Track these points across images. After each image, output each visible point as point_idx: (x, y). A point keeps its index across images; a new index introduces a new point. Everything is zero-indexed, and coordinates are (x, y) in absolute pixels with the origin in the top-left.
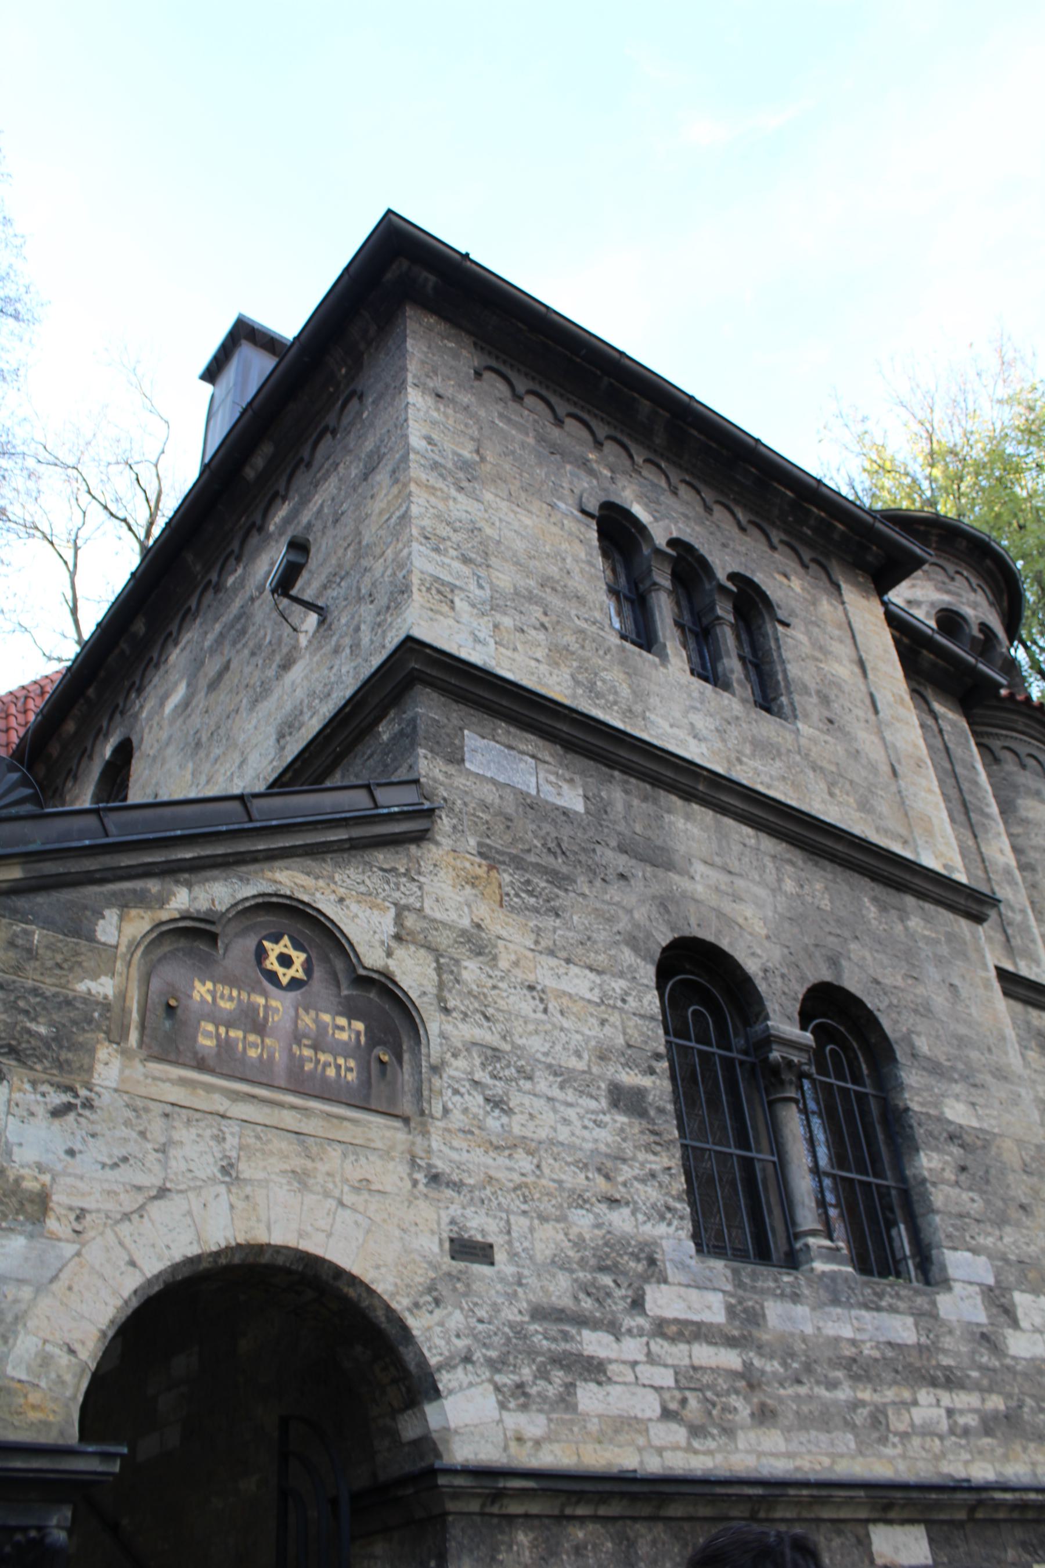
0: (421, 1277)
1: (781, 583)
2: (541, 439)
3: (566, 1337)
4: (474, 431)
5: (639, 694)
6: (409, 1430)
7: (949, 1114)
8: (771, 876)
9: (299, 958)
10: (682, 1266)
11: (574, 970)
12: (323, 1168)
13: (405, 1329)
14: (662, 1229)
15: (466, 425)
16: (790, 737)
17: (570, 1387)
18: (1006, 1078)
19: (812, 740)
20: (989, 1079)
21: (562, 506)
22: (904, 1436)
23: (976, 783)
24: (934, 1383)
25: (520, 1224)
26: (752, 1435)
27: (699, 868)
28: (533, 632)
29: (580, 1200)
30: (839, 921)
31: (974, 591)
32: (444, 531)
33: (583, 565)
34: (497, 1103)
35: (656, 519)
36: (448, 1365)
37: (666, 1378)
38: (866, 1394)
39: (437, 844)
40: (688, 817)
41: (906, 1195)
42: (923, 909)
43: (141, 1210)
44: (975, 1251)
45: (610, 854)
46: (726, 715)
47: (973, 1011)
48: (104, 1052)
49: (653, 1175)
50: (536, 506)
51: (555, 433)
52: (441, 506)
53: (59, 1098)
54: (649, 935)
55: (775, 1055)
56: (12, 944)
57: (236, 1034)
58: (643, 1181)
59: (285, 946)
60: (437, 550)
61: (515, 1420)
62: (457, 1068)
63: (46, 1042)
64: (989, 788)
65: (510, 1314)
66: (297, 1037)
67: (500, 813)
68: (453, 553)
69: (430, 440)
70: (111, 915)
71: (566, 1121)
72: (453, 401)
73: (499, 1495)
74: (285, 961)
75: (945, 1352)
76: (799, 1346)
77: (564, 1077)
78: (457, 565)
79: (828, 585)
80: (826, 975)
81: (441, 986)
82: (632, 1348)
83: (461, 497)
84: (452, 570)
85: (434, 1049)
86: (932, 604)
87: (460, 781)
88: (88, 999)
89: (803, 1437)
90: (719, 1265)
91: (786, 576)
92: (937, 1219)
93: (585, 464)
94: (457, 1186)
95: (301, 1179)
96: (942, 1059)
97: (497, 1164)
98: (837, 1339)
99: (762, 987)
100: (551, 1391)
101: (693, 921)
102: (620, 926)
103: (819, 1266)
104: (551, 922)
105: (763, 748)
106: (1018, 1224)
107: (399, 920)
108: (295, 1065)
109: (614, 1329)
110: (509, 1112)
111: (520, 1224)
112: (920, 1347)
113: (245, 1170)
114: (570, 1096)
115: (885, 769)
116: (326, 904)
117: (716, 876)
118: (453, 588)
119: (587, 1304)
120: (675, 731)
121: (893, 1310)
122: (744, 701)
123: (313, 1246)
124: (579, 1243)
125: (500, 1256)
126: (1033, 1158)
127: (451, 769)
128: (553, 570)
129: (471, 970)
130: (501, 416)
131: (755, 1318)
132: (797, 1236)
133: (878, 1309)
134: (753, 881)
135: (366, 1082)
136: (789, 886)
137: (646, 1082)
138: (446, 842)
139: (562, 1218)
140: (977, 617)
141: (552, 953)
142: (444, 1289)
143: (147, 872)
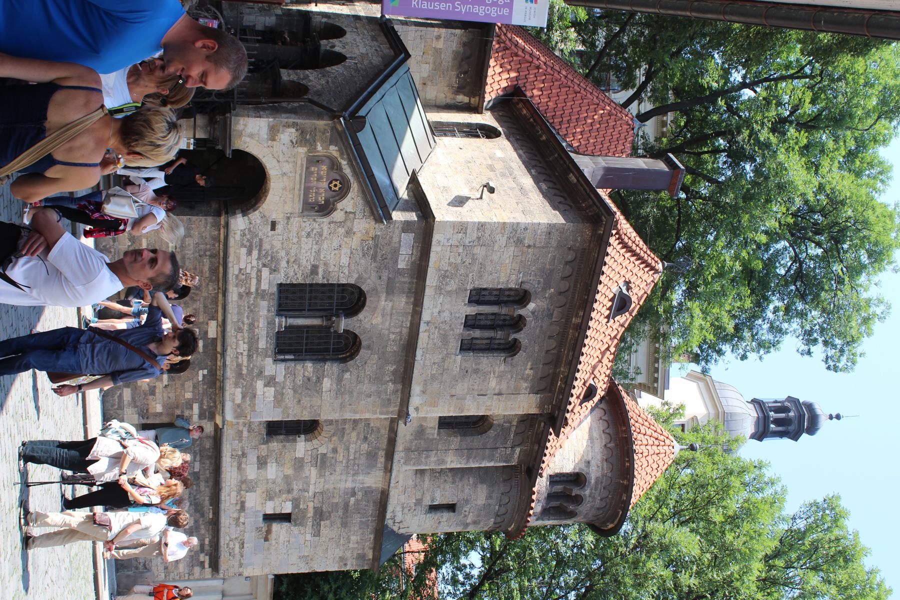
0: (266, 214)
1: (527, 364)
2: (552, 271)
3: (256, 247)
4: (538, 245)
5: (449, 293)
6: (237, 211)
8: (393, 330)
9: (337, 189)
10: (274, 279)
11: (348, 259)
12: (288, 193)
13: (255, 210)
14: (283, 275)
15: (540, 242)
16: (453, 351)
17: (245, 246)
18: (341, 409)
19: (455, 361)
20: (340, 401)
21: (521, 275)
22: (236, 338)
23: (483, 459)
25: (280, 238)
26: (236, 292)
27: (390, 304)
28: (460, 258)
29: (288, 254)
30: (383, 353)
31: (601, 500)
32: (488, 232)
33: (496, 280)
34: (308, 235)
35: (533, 313)
36: (249, 219)
37: (248, 271)
38: (246, 327)
39: (376, 224)
40: (407, 303)
41: (302, 360)
42: (397, 391)
43: (274, 158)
44: (285, 377)
45: (387, 274)
46: (453, 326)
47: (363, 402)
48: (305, 149)
49: (296, 274)
50: (517, 266)
51: (557, 276)
52: (498, 231)
53: (294, 141)
54: (363, 283)
55: (334, 318)
56: (325, 130)
57: (316, 175)
58: (294, 271)
59: (339, 186)
60: (478, 229)
61: (239, 233)
62: (316, 225)
63: (305, 138)
64: (483, 465)
65: (260, 234)
66: (317, 188)
67: (390, 242)
68: (480, 234)
69: (526, 229)
70: (337, 148)
71: (307, 252)
72: (549, 238)
73: (224, 227)
74: (336, 186)
75: (257, 357)
76: (257, 309)
77: (318, 252)
79: (536, 389)
80: (364, 343)
81: (336, 222)
82: (255, 263)
83: (505, 238)
85: (320, 220)
86: (588, 473)
87: (397, 232)
88: (316, 145)
89: (236, 306)
90: (274, 289)
91: (531, 369)
92: (293, 365)
93: (547, 286)
94: (287, 224)
95: (285, 189)
96: (343, 383)
97: (293, 234)
98: (259, 322)
99: (355, 318)
100: (245, 242)
101: (372, 299)
102: (364, 274)
103: (277, 320)
104: (361, 254)
105: (444, 338)
106: (294, 397)
107: (350, 213)
108: (312, 188)
109: (259, 259)
110: (307, 237)
111: (280, 238)
112: (258, 348)
113: (285, 177)
114: (313, 254)
115: (453, 392)
117: (389, 309)
118: (465, 233)
119: (264, 253)
120: (440, 305)
121: (267, 342)
122: (462, 334)
123: (271, 192)
124: (277, 252)
125: (273, 232)
126: (315, 410)
127: (400, 229)
128: (489, 268)
129: (341, 231)
130: (555, 256)
131: (263, 298)
132: (286, 317)
133: (267, 337)
134: (390, 323)
135: (310, 204)
136: (392, 337)
137: (320, 276)
138: (377, 226)
139: (283, 249)
140: (585, 495)
141: (351, 253)
142: (265, 219)
143: (348, 155)
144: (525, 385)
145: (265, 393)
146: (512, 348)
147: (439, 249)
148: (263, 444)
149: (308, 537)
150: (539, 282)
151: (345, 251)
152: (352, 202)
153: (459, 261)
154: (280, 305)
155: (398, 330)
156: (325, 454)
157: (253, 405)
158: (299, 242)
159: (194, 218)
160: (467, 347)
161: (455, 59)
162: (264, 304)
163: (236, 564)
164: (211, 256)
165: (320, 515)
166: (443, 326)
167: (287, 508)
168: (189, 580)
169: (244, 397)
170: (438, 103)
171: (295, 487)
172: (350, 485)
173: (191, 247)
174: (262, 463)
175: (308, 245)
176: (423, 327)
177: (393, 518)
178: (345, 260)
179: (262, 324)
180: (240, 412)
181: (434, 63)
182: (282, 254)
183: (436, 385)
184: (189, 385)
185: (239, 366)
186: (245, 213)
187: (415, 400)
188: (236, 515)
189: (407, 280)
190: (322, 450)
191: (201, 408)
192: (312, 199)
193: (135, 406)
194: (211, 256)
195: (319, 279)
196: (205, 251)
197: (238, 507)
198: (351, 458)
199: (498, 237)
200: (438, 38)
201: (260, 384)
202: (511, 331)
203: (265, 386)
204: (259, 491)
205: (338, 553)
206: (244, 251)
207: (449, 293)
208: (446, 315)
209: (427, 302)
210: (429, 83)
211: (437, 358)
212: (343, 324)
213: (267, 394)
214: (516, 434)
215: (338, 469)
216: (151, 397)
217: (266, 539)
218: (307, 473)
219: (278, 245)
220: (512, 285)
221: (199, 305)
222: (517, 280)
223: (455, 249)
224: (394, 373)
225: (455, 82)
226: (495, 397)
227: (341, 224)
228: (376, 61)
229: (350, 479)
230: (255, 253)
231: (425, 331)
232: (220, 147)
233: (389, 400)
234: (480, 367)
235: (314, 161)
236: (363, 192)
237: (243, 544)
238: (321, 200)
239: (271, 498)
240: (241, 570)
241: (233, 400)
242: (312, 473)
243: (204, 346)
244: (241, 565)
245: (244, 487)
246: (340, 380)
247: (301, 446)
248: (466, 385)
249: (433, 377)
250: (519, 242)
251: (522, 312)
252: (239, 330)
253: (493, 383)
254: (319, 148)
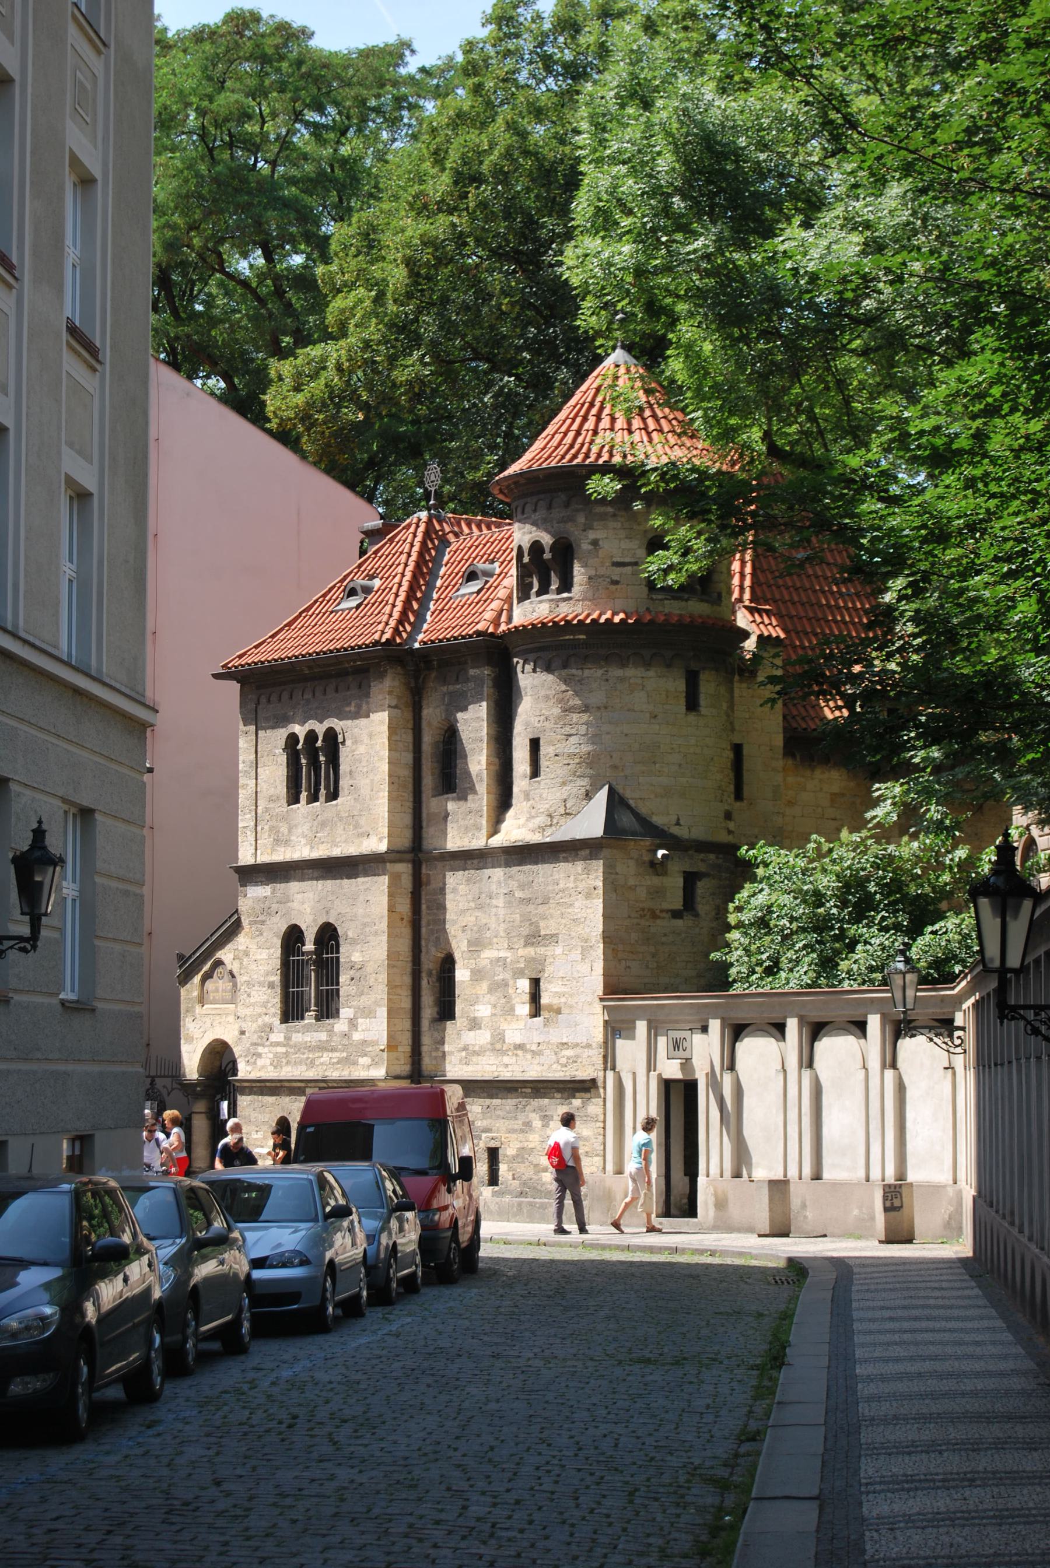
20: (371, 938)
29: (260, 1015)
77: (261, 984)
82: (266, 1050)
109: (263, 1045)
149: (559, 950)
157: (374, 1043)
158: (253, 1005)
160: (333, 795)
163: (587, 1052)
165: (534, 938)
167: (524, 985)
168: (604, 1122)
171: (501, 977)
172: (500, 902)
174: (474, 1024)
177: (542, 829)
178: (263, 955)
183: (363, 821)
188: (529, 1056)
195: (276, 978)
197: (520, 1052)
198: (472, 905)
201: (357, 1036)
204: (504, 1026)
205: (580, 902)
207: (290, 831)
215: (484, 921)
217: (559, 1011)
218: (487, 961)
219: (255, 1025)
229: (494, 902)
230: (260, 1049)
237: (563, 1044)
239: (512, 1009)
240: (594, 1045)
242: (488, 954)
244: (589, 1046)
245: (498, 1046)
246: (354, 942)
247: (461, 974)
253: (362, 749)
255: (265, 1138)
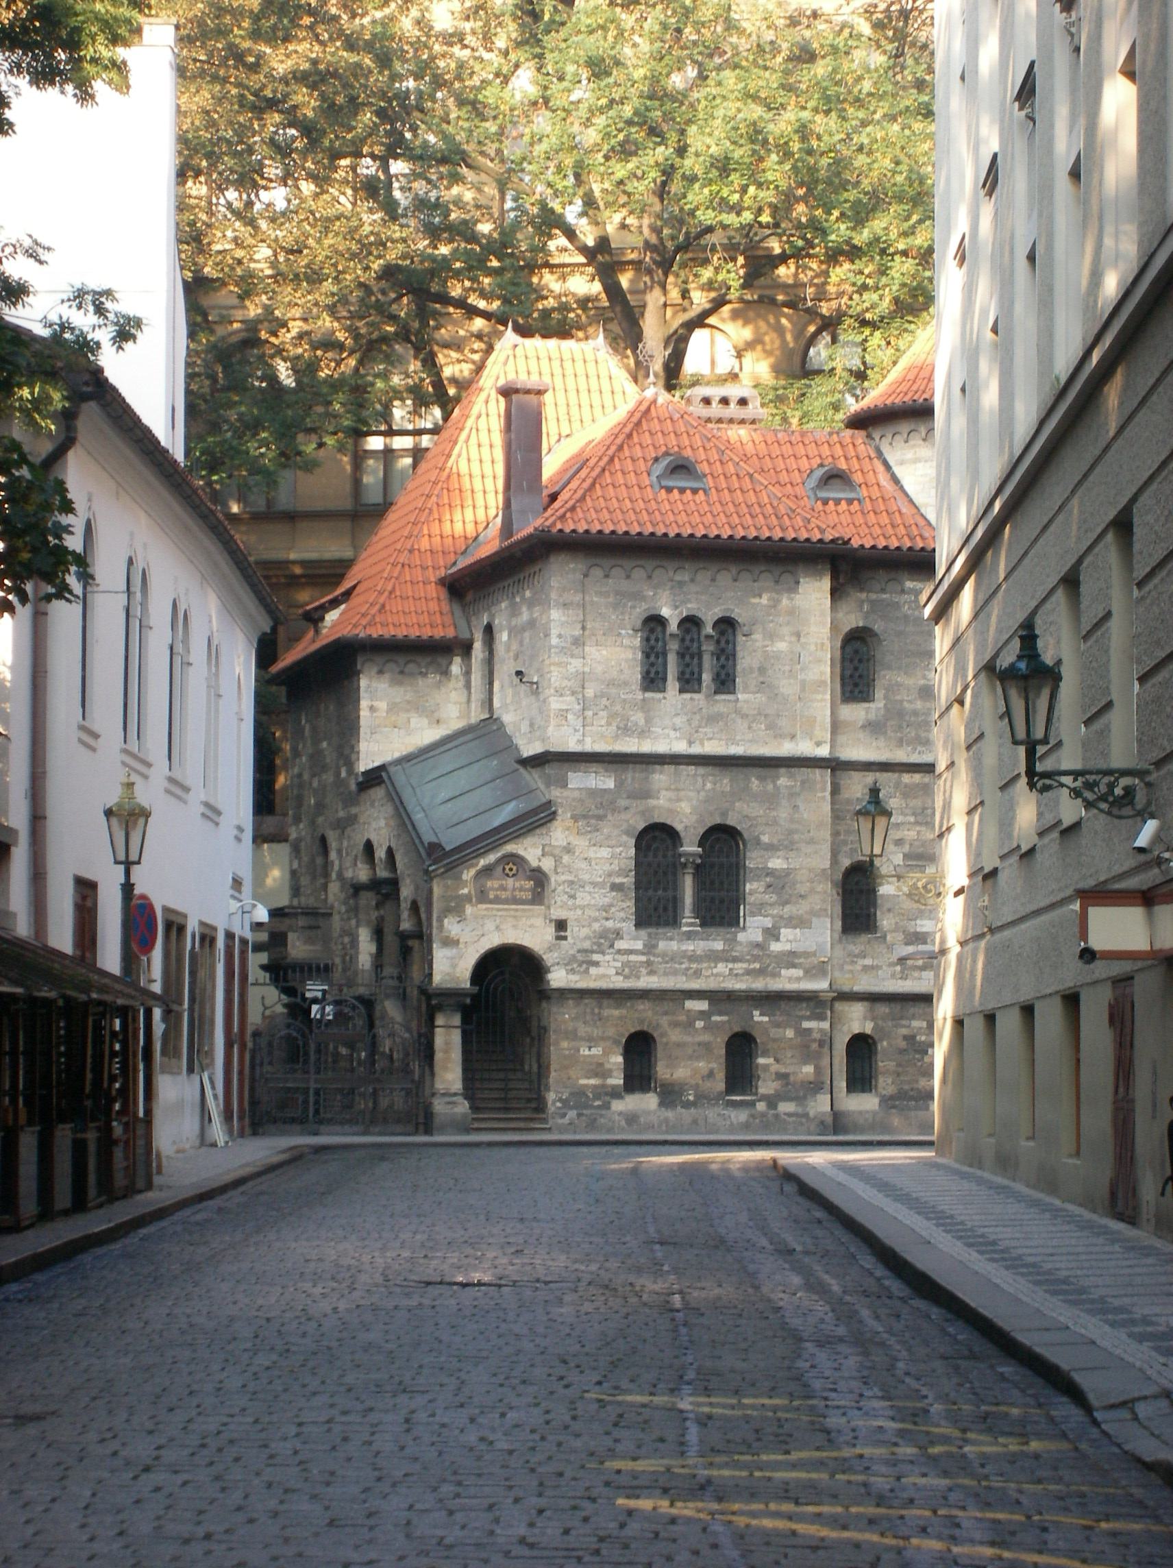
2: (617, 593)
5: (648, 720)
7: (770, 865)
19: (746, 702)
24: (727, 961)
27: (663, 793)
29: (596, 920)
32: (566, 683)
34: (573, 897)
35: (676, 607)
38: (694, 966)
51: (625, 585)
69: (560, 636)
77: (595, 884)
78: (569, 699)
80: (718, 821)
82: (608, 958)
84: (569, 702)
85: (553, 884)
87: (566, 793)
90: (643, 933)
93: (638, 596)
95: (515, 927)
99: (682, 834)
103: (685, 929)
105: (712, 719)
109: (603, 953)
116: (521, 852)
129: (566, 859)
131: (655, 946)
136: (709, 786)
144: (785, 602)
145: (789, 940)
146: (727, 625)
147: (588, 740)
148: (884, 937)
150: (633, 607)
151: (592, 853)
152: (530, 850)
153: (604, 714)
154: (667, 924)
155: (700, 780)
156: (906, 856)
157: (806, 954)
158: (583, 908)
159: (553, 1026)
161: (400, 683)
162: (662, 945)
164: (600, 1007)
166: (695, 723)
169: (794, 966)
170: (464, 699)
173: (589, 1029)
175: (583, 898)
176: (696, 750)
178: (605, 853)
179: (689, 946)
180: (819, 970)
181: (408, 711)
182: (596, 926)
183: (783, 722)
184: (774, 1032)
185: (748, 972)
186: (548, 971)
187: (805, 748)
189: (629, 775)
190: (898, 859)
191: (809, 1018)
192: (529, 895)
193: (805, 1097)
194: (600, 1007)
195: (629, 880)
196: (593, 1013)
198: (912, 819)
199: (571, 669)
200: (372, 708)
201: (775, 947)
202: (704, 633)
203: (778, 939)
206: (593, 970)
207: (648, 720)
208: (678, 721)
209: (661, 747)
210: (436, 715)
211: (741, 725)
212: (690, 847)
213: (791, 937)
214: (883, 591)
216: (792, 1078)
219: (585, 931)
220: (637, 641)
221: (664, 1021)
222: (630, 636)
223: (589, 721)
224: (762, 779)
225: (433, 678)
226: (803, 640)
227: (558, 860)
228: (389, 809)
230: (596, 957)
231: (702, 744)
232: (468, 1001)
233: (803, 782)
234: (756, 664)
235: (482, 896)
236: (517, 836)
238: (530, 884)
241: (798, 979)
243: (720, 1014)
246: (771, 848)
248: (784, 682)
249: (768, 728)
250: (578, 642)
251: (673, 627)
252: (697, 974)
253: (781, 646)
254: (465, 891)
255: (606, 1053)
